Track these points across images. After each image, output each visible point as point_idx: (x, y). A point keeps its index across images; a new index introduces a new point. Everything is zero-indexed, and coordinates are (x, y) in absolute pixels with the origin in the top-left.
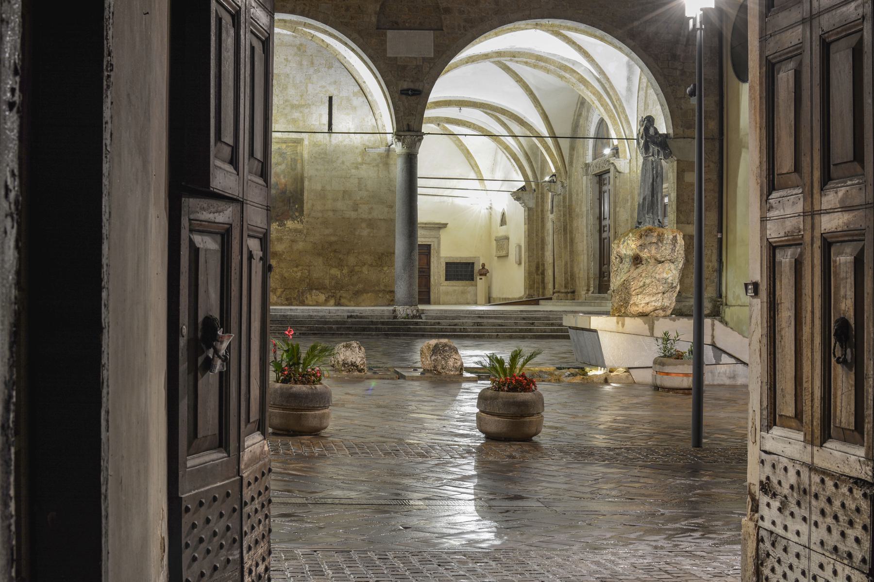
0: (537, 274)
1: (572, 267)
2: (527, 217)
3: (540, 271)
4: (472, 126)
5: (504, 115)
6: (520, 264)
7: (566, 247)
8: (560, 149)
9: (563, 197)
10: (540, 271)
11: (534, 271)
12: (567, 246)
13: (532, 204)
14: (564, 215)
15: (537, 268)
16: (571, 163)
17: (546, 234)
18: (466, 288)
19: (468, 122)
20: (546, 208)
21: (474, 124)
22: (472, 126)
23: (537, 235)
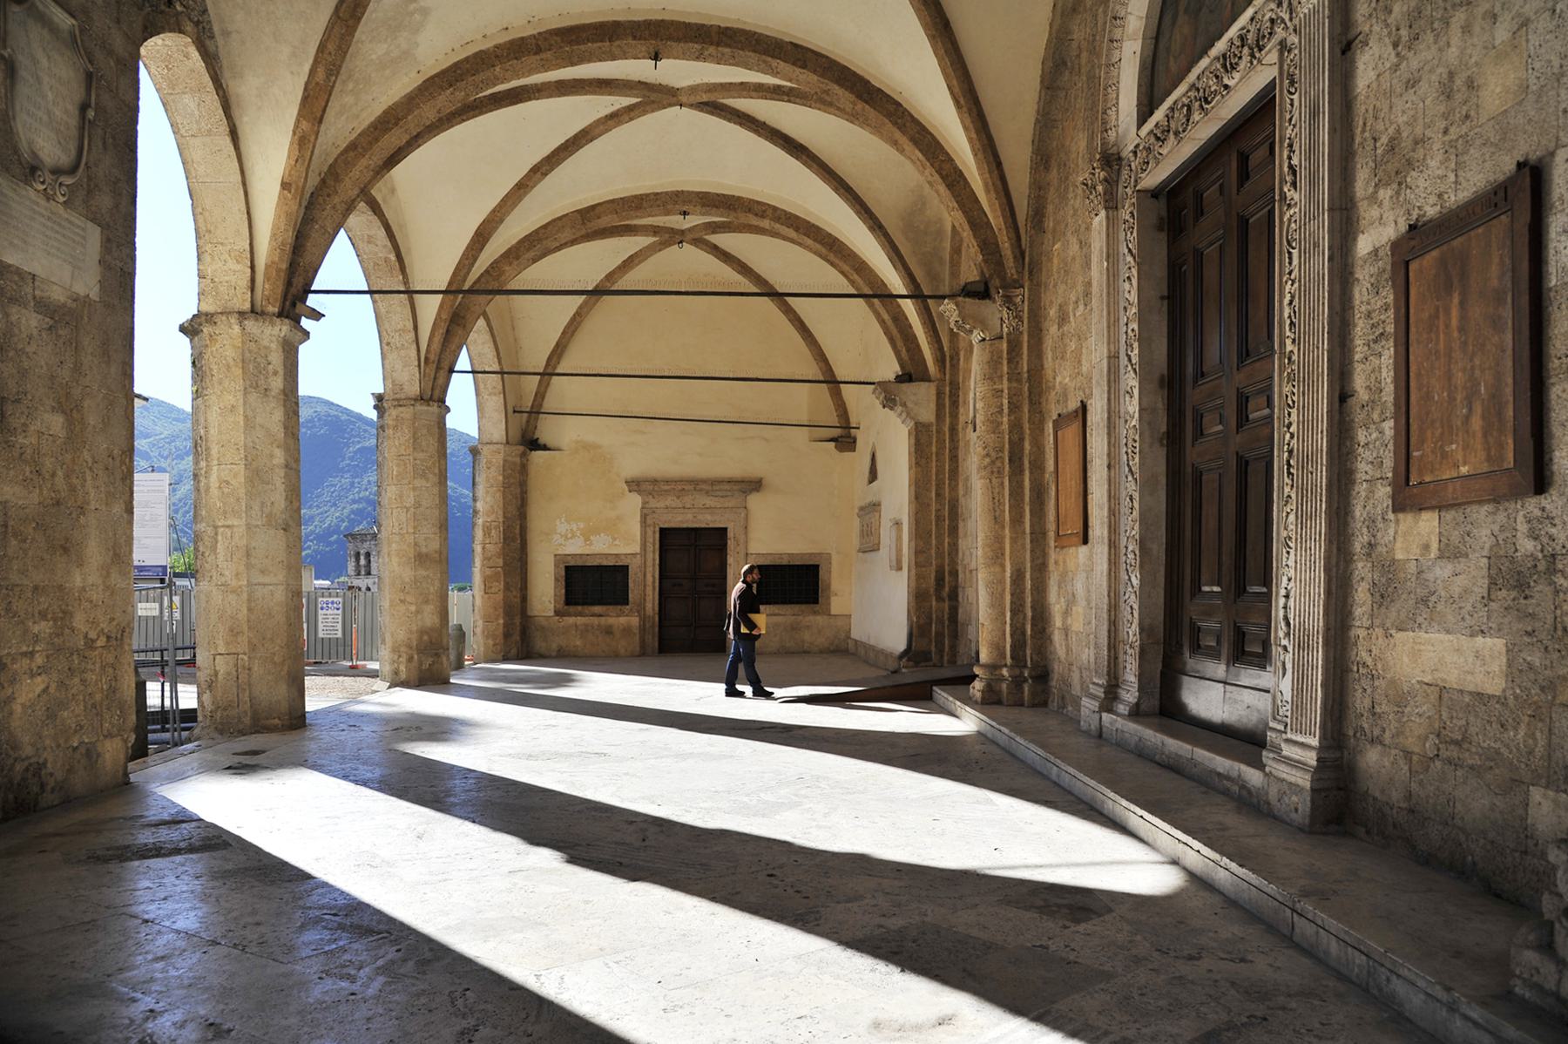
0: (940, 599)
1: (1040, 589)
2: (913, 449)
3: (947, 589)
4: (769, 212)
5: (804, 67)
6: (900, 568)
7: (1017, 520)
8: (999, 165)
9: (1009, 342)
10: (947, 589)
11: (932, 591)
12: (1022, 516)
13: (927, 414)
14: (1014, 407)
15: (940, 580)
16: (1038, 215)
17: (961, 492)
18: (800, 618)
19: (758, 203)
20: (962, 419)
21: (775, 209)
22: (769, 212)
23: (938, 495)
